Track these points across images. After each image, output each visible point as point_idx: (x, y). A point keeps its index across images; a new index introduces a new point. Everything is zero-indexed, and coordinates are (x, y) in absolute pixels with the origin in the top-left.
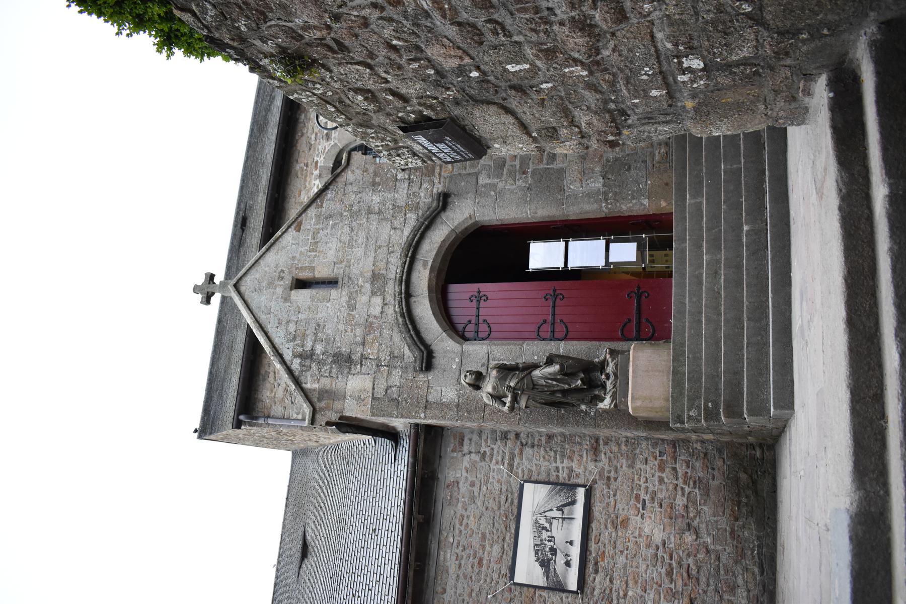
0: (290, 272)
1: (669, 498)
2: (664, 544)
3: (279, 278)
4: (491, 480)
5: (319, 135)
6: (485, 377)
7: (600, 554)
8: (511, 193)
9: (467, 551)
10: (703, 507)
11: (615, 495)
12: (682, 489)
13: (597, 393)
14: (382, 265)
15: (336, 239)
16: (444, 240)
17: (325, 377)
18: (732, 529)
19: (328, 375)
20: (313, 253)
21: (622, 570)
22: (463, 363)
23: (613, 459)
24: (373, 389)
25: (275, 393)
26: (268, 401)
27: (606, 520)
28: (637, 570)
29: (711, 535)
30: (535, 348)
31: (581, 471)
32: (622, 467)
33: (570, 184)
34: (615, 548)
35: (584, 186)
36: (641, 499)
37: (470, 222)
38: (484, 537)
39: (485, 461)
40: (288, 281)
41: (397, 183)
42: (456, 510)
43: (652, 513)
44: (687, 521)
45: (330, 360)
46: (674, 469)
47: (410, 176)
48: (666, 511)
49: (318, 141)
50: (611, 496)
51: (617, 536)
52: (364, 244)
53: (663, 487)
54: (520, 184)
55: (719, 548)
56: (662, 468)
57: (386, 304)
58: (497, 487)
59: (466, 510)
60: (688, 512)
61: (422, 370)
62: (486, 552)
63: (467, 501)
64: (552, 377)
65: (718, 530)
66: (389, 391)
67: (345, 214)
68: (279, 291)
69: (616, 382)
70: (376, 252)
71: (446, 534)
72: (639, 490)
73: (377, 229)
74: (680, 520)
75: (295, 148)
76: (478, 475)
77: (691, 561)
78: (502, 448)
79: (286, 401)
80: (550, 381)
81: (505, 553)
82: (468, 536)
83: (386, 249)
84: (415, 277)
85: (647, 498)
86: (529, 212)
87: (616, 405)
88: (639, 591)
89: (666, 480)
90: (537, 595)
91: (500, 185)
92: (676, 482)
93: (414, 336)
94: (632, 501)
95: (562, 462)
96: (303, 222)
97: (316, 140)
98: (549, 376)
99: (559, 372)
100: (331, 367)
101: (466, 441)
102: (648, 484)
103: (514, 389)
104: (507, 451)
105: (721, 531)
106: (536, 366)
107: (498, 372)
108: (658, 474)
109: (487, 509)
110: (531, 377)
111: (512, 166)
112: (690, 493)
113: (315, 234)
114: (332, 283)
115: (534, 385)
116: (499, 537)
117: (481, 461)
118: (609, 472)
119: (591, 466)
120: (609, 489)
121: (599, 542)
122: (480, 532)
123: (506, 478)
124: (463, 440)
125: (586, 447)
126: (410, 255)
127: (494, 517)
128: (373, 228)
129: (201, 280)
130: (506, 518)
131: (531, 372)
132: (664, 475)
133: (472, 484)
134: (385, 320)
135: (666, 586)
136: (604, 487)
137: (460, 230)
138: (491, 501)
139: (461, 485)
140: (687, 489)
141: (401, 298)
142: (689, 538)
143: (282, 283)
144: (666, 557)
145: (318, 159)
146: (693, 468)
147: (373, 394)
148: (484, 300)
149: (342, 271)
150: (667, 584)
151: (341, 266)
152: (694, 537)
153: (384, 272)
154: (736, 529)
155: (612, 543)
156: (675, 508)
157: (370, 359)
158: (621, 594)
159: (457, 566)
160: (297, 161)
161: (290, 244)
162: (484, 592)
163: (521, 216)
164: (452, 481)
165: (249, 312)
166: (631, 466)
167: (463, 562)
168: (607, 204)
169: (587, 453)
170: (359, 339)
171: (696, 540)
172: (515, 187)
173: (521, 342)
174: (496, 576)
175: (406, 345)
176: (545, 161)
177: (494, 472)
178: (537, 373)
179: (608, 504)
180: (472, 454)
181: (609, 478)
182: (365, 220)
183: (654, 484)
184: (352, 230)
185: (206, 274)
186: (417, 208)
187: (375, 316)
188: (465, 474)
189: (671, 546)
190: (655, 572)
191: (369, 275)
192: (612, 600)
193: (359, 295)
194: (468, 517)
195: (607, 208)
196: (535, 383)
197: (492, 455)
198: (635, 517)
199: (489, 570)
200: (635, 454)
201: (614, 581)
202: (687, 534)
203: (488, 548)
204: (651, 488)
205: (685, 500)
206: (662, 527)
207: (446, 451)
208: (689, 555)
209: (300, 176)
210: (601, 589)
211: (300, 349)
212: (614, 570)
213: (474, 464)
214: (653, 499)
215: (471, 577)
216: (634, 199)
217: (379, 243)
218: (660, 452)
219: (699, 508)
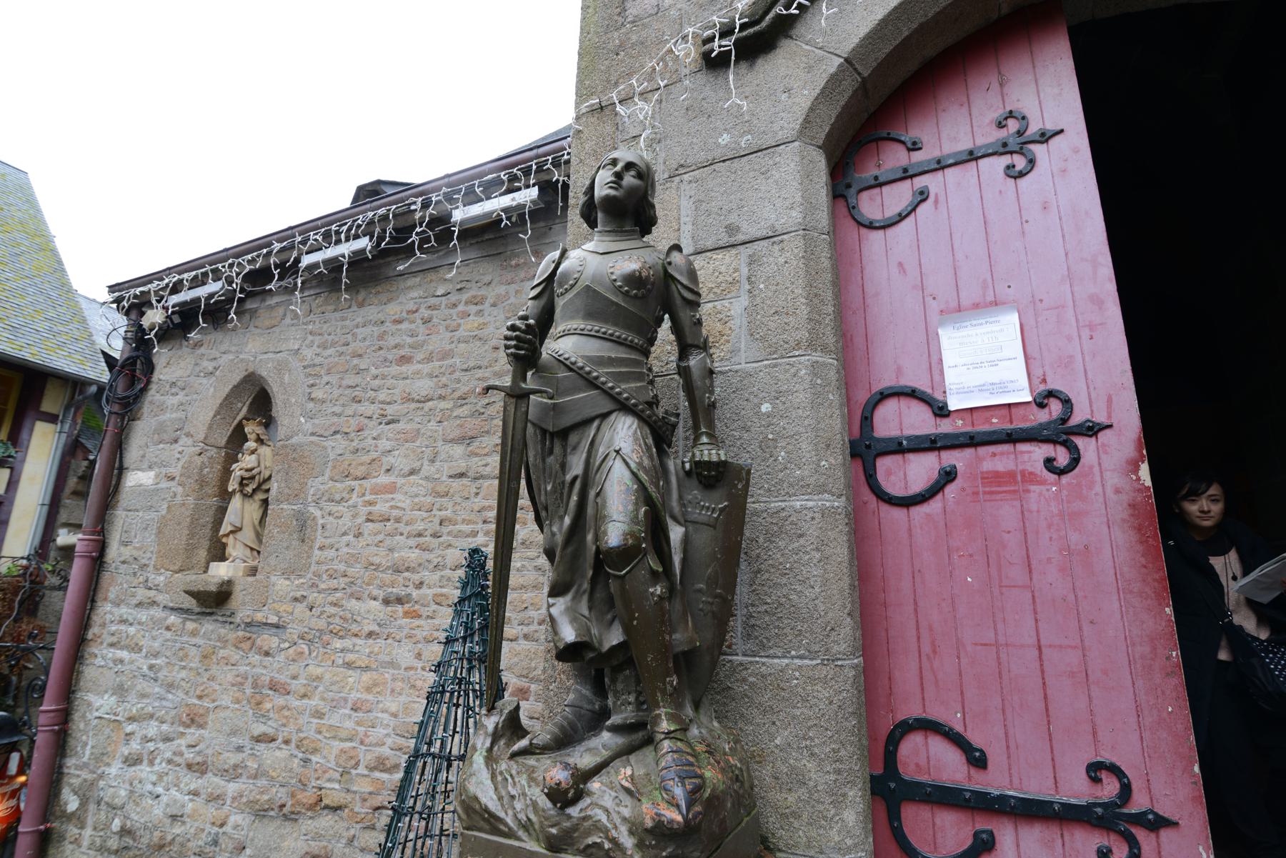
7: (417, 607)
9: (422, 329)
11: (526, 637)
21: (387, 659)
22: (736, 163)
28: (388, 693)
30: (801, 397)
38: (446, 355)
42: (493, 284)
50: (526, 629)
59: (494, 305)
63: (509, 302)
80: (575, 498)
82: (448, 322)
88: (354, 695)
90: (353, 483)
98: (592, 494)
110: (604, 416)
115: (564, 434)
121: (437, 603)
127: (480, 367)
135: (361, 756)
148: (1010, 167)
150: (366, 757)
158: (350, 657)
159: (397, 317)
162: (358, 379)
167: (404, 326)
173: (830, 339)
174: (382, 396)
190: (385, 732)
192: (341, 638)
194: (480, 313)
196: (573, 438)
199: (392, 381)
201: (371, 641)
203: (426, 368)
210: (359, 614)
212: (390, 641)
215: (381, 348)
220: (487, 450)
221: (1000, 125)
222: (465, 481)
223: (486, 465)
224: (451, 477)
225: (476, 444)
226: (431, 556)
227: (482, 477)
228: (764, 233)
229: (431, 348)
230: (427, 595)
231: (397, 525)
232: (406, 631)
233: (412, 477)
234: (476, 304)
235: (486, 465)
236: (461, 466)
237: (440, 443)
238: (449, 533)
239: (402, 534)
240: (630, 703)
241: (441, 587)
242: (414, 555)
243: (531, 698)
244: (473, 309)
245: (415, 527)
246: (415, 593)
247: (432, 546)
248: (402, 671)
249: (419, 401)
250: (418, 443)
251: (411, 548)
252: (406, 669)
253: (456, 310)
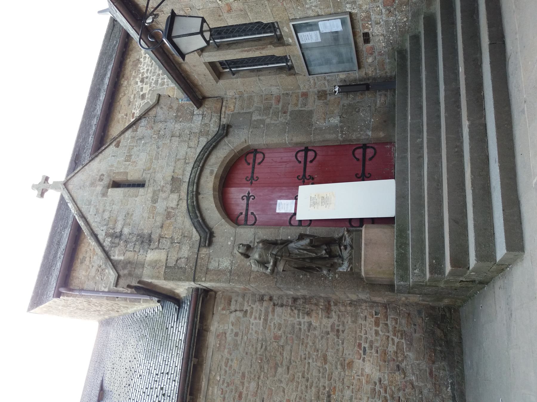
0: (109, 176)
1: (383, 346)
2: (380, 381)
3: (99, 180)
4: (250, 331)
5: (136, 95)
6: (253, 248)
7: (332, 388)
8: (275, 126)
9: (231, 387)
10: (408, 354)
12: (393, 339)
13: (336, 261)
14: (179, 172)
15: (146, 154)
16: (226, 156)
17: (129, 251)
18: (430, 370)
19: (132, 250)
20: (127, 163)
23: (341, 316)
24: (167, 260)
25: (89, 272)
26: (83, 278)
27: (336, 362)
29: (416, 375)
31: (317, 325)
32: (347, 322)
33: (317, 121)
34: (343, 384)
35: (327, 122)
36: (363, 347)
37: (245, 145)
38: (243, 375)
39: (246, 317)
40: (106, 181)
41: (194, 117)
43: (371, 357)
44: (397, 364)
45: (134, 239)
46: (386, 325)
47: (203, 112)
48: (381, 355)
49: (136, 99)
50: (340, 344)
51: (345, 375)
52: (167, 157)
53: (378, 338)
54: (281, 120)
55: (421, 384)
56: (377, 324)
57: (181, 199)
58: (255, 336)
59: (231, 354)
60: (397, 357)
61: (205, 246)
62: (245, 388)
64: (304, 248)
65: (420, 370)
66: (179, 261)
67: (155, 136)
68: (99, 189)
69: (352, 252)
70: (175, 163)
71: (214, 374)
72: (361, 339)
73: (177, 147)
74: (391, 363)
75: (118, 103)
76: (241, 327)
77: (401, 394)
78: (259, 307)
79: (97, 278)
80: (302, 251)
81: (259, 389)
83: (184, 161)
84: (202, 181)
85: (367, 346)
87: (351, 269)
89: (380, 332)
91: (268, 121)
92: (388, 334)
93: (201, 221)
94: (356, 348)
95: (304, 318)
96: (122, 141)
97: (134, 99)
98: (302, 247)
99: (309, 244)
100: (135, 244)
101: (233, 302)
102: (367, 336)
103: (276, 255)
104: (263, 309)
105: (422, 371)
106: (291, 241)
107: (263, 244)
108: (374, 328)
109: (247, 353)
111: (276, 108)
112: (398, 343)
113: (130, 149)
114: (141, 185)
115: (290, 254)
116: (255, 376)
117: (244, 317)
118: (338, 326)
119: (325, 321)
120: (339, 338)
121: (331, 379)
122: (241, 372)
123: (262, 330)
124: (231, 301)
125: (321, 307)
126: (201, 165)
127: (252, 360)
128: (174, 146)
129: (38, 180)
130: (261, 361)
131: (288, 244)
132: (379, 329)
133: (236, 334)
134: (180, 210)
136: (335, 337)
138: (250, 347)
139: (228, 335)
140: (396, 340)
141: (193, 194)
142: (398, 376)
143: (101, 183)
144: (382, 391)
145: (135, 111)
146: (401, 324)
147: (166, 264)
148: (253, 199)
149: (149, 175)
151: (148, 172)
152: (403, 376)
153: (180, 177)
154: (434, 370)
155: (341, 380)
156: (388, 354)
157: (166, 238)
159: (222, 399)
160: (119, 112)
161: (111, 156)
163: (281, 142)
164: (221, 332)
165: (74, 203)
166: (354, 322)
167: (227, 396)
168: (343, 134)
169: (322, 312)
170: (158, 224)
171: (404, 378)
172: (277, 122)
173: (278, 227)
175: (194, 228)
176: (300, 106)
177: (253, 325)
178: (292, 245)
179: (338, 350)
180: (237, 312)
181: (338, 331)
182: (169, 141)
183: (371, 336)
184: (158, 148)
185: (43, 176)
186: (207, 134)
187: (172, 208)
188: (231, 327)
189: (385, 383)
191: (169, 179)
193: (161, 193)
194: (232, 360)
195: (342, 137)
196: (291, 252)
197: (252, 313)
198: (358, 360)
200: (357, 313)
202: (397, 373)
203: (246, 384)
204: (370, 338)
205: (395, 347)
206: (378, 368)
207: (217, 309)
208: (399, 390)
209: (121, 122)
211: (111, 231)
213: (238, 319)
214: (371, 347)
216: (362, 131)
217: (178, 157)
218: (375, 312)
219: (406, 354)
220: (281, 358)
221: (244, 199)
222: (290, 367)
223: (286, 358)
224: (288, 373)
225: (278, 362)
226: (315, 382)
227: (290, 360)
228: (254, 236)
229: (239, 383)
230: (328, 384)
231: (302, 398)
232: (340, 394)
233: (286, 392)
234: (228, 362)
235: (286, 358)
236: (285, 368)
237: (275, 378)
238: (308, 374)
239: (306, 396)
241: (325, 378)
242: (313, 389)
243: (361, 342)
244: (230, 363)
245: (304, 389)
246: (327, 389)
247: (311, 381)
248: (353, 394)
249: (258, 388)
250: (273, 389)
251: (311, 391)
252: (353, 393)
253: (228, 371)
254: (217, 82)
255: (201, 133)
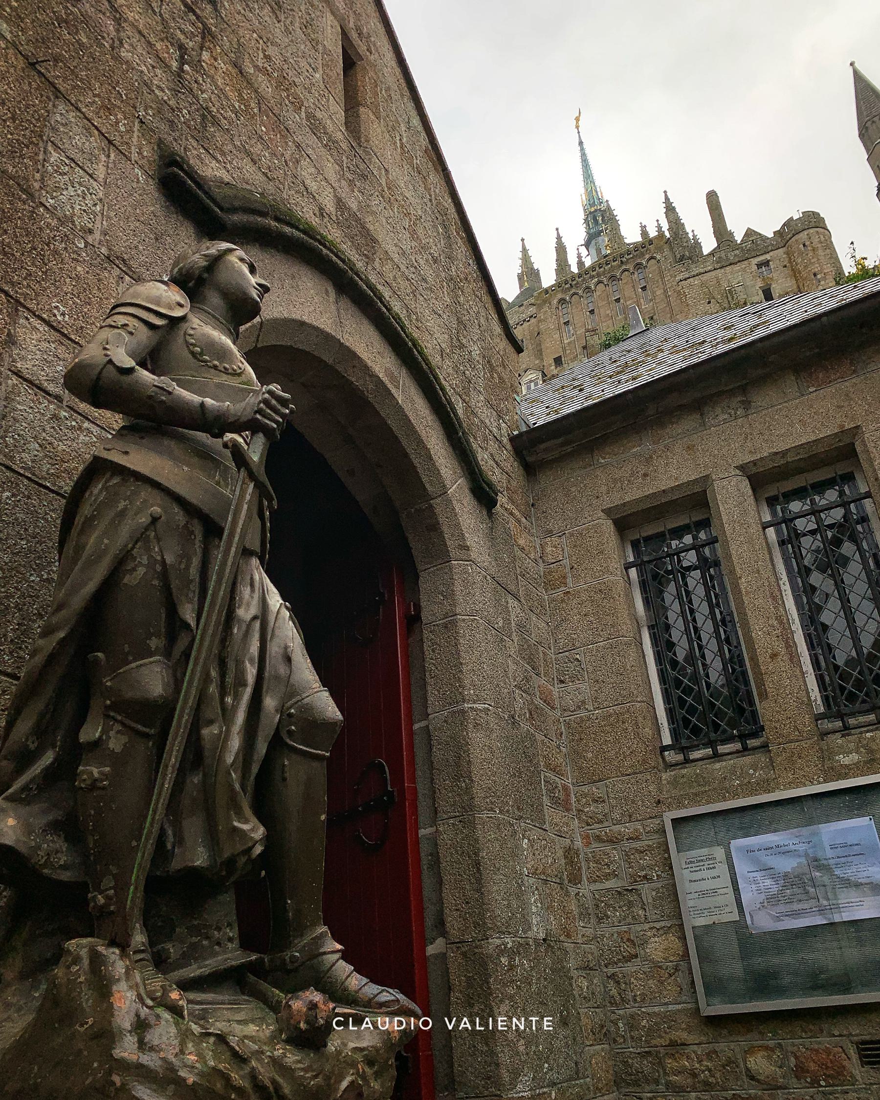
86: (480, 706)
137: (438, 510)
195: (502, 950)
240: (230, 940)
254: (608, 512)
255: (470, 411)
